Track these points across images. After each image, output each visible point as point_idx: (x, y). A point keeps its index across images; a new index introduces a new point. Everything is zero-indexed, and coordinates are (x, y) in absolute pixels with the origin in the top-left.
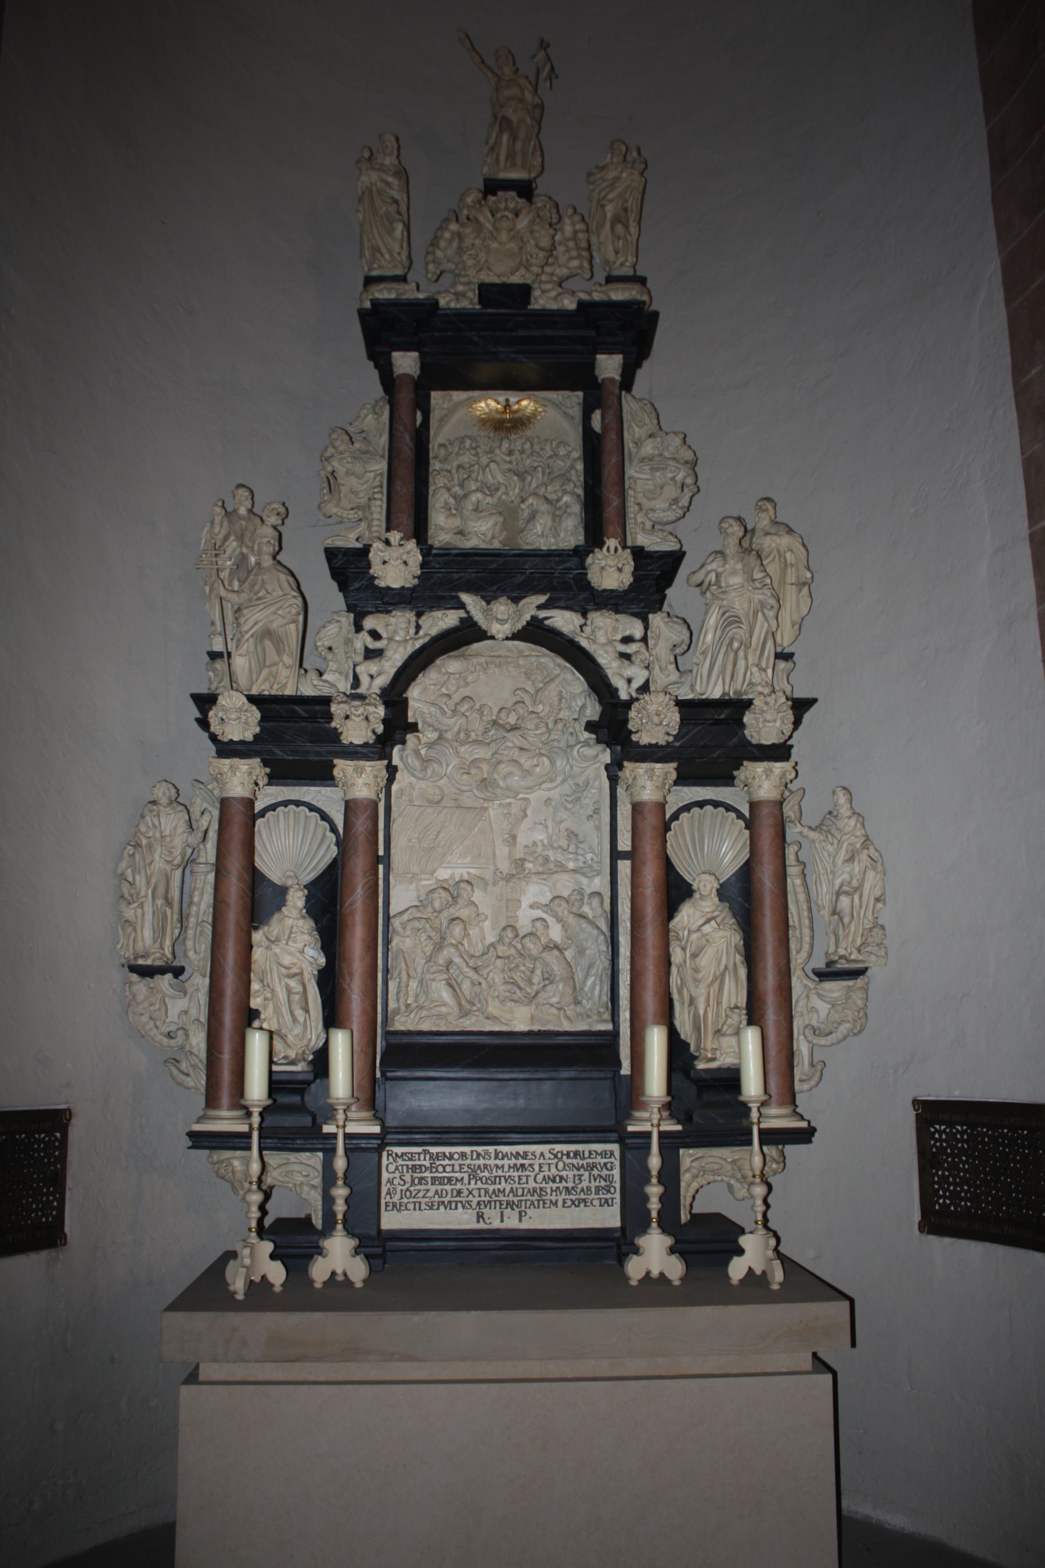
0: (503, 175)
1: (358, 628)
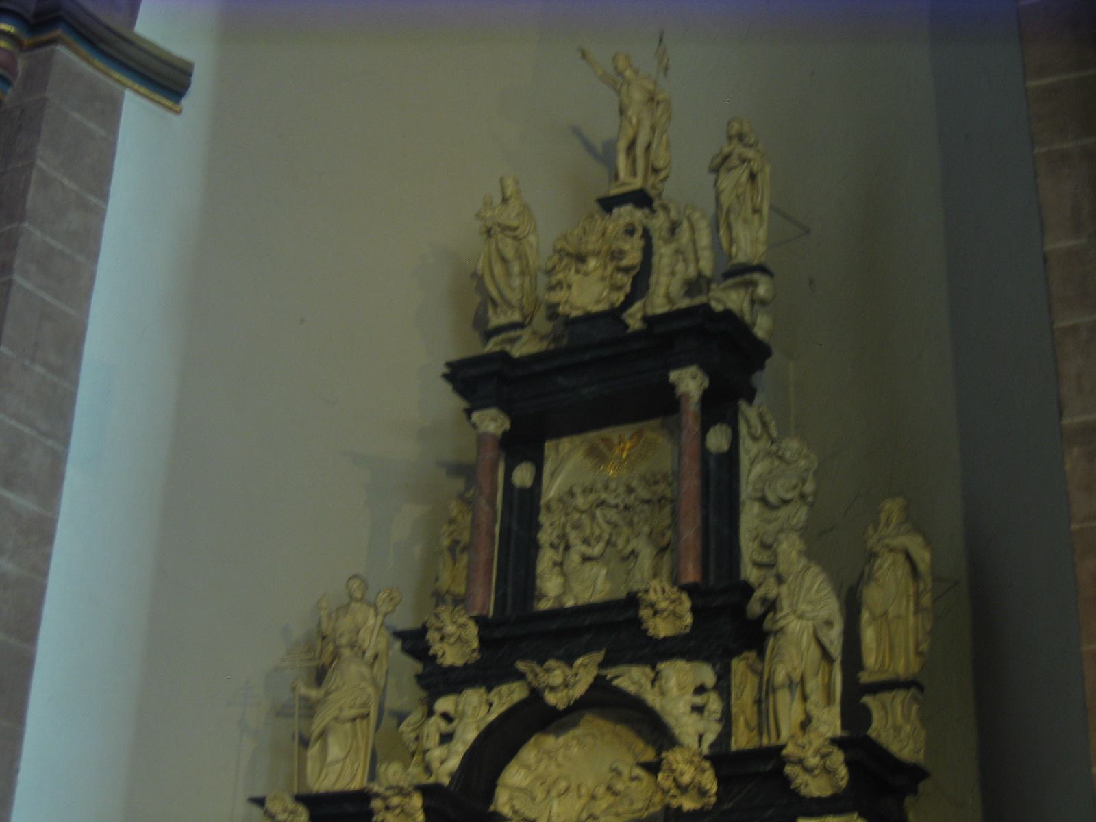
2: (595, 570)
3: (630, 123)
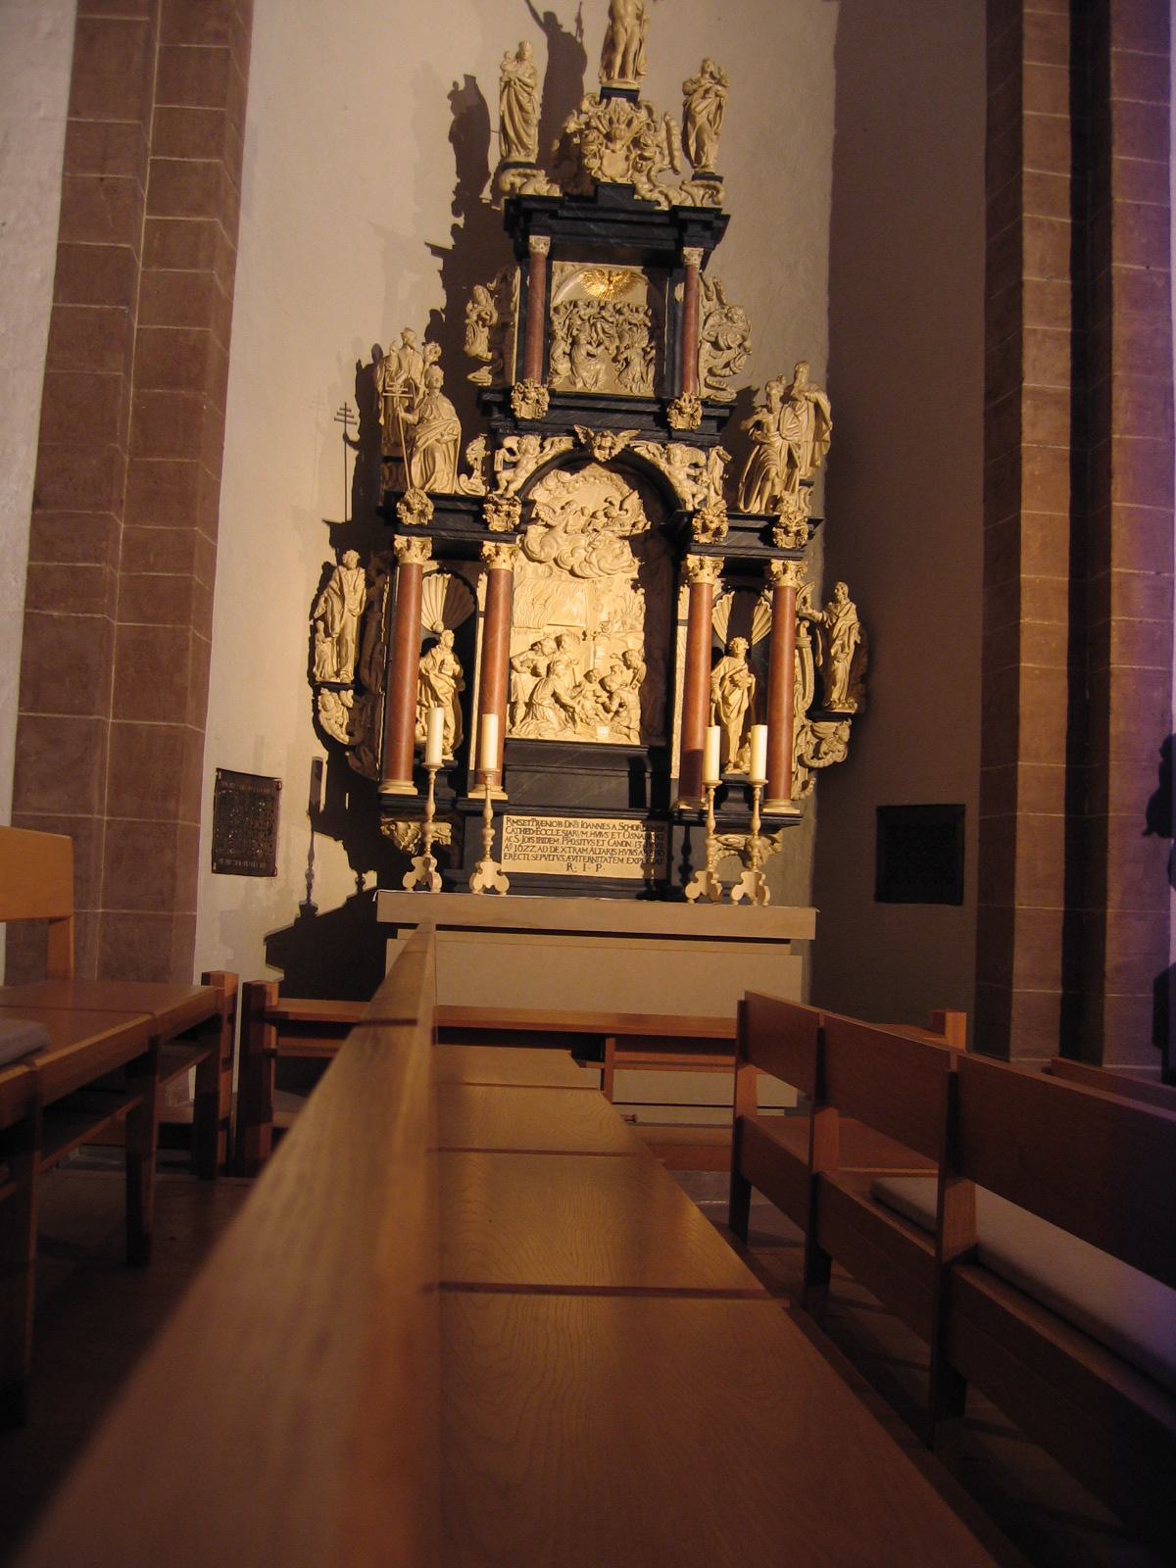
0: (615, 86)
2: (598, 367)
3: (626, 30)
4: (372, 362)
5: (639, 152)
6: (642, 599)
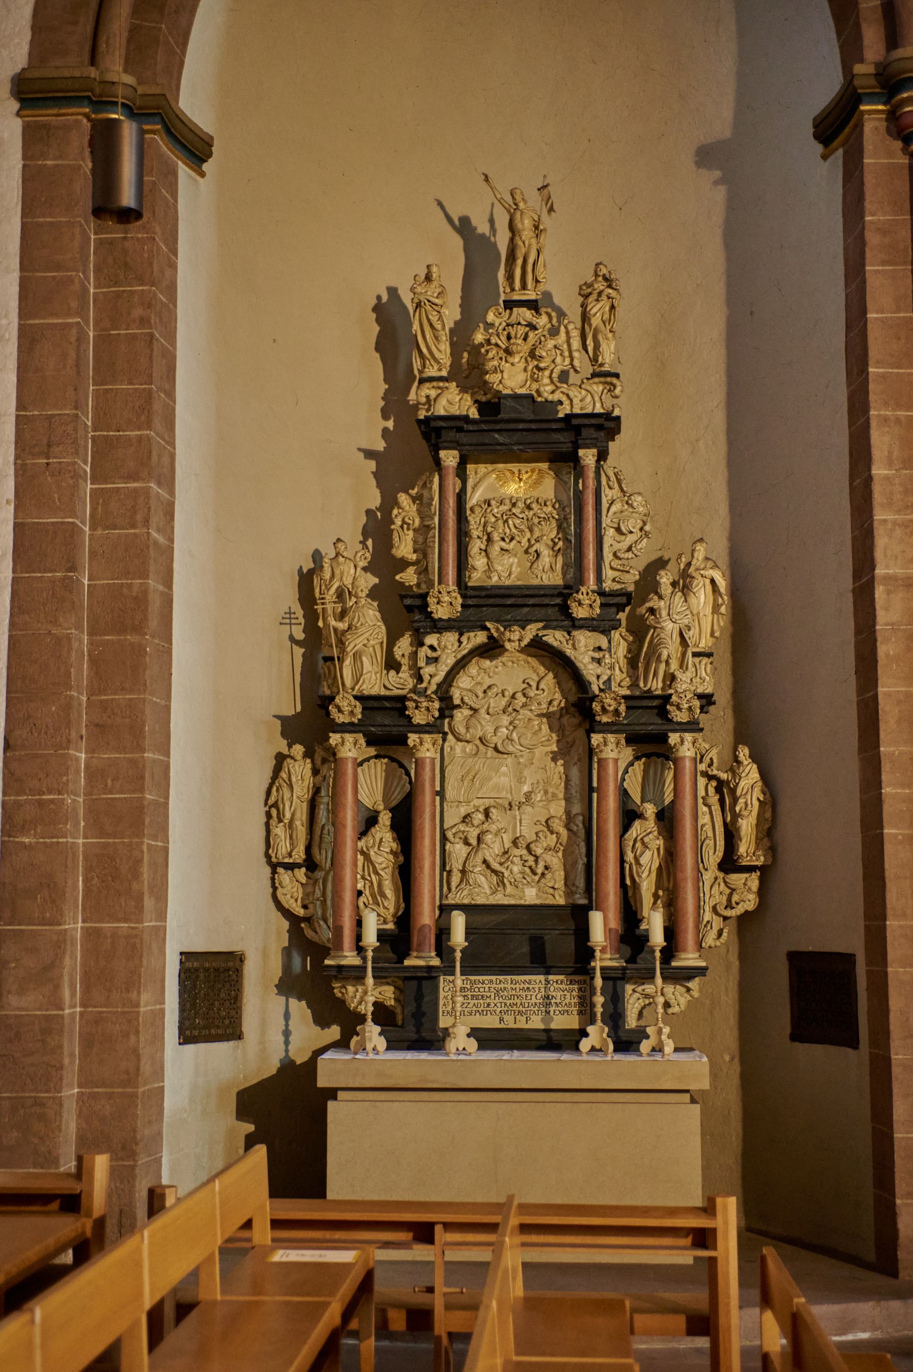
0: (516, 297)
1: (422, 644)
2: (511, 560)
3: (524, 243)
4: (312, 566)
5: (536, 363)
6: (562, 769)
